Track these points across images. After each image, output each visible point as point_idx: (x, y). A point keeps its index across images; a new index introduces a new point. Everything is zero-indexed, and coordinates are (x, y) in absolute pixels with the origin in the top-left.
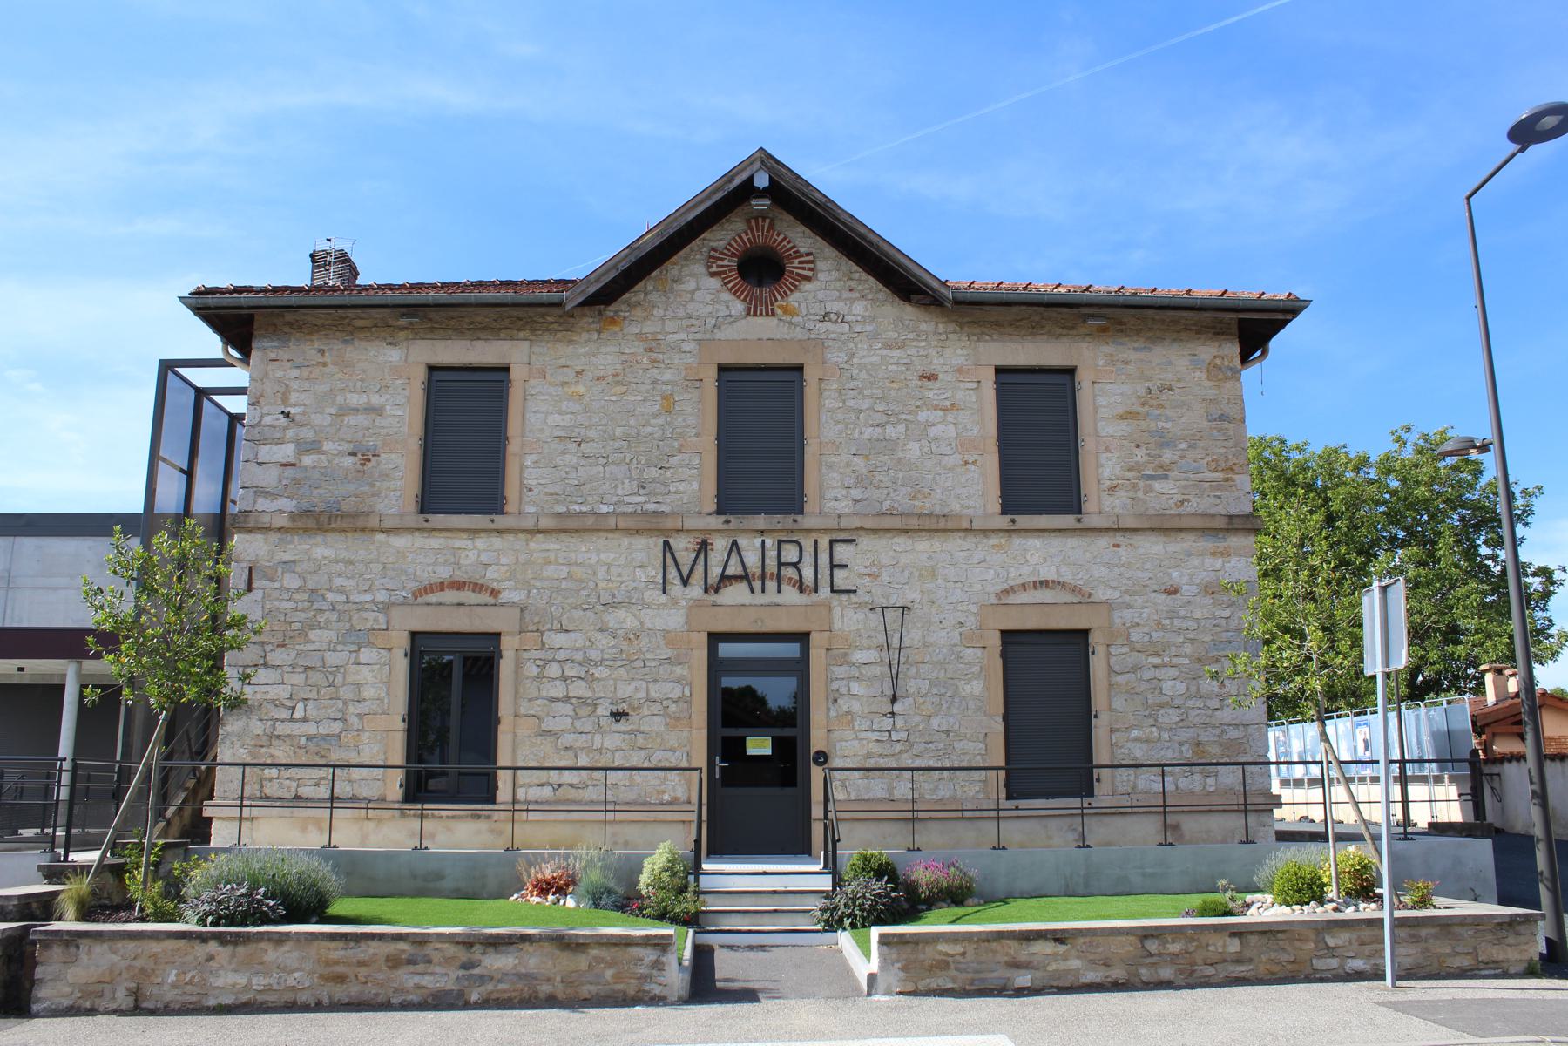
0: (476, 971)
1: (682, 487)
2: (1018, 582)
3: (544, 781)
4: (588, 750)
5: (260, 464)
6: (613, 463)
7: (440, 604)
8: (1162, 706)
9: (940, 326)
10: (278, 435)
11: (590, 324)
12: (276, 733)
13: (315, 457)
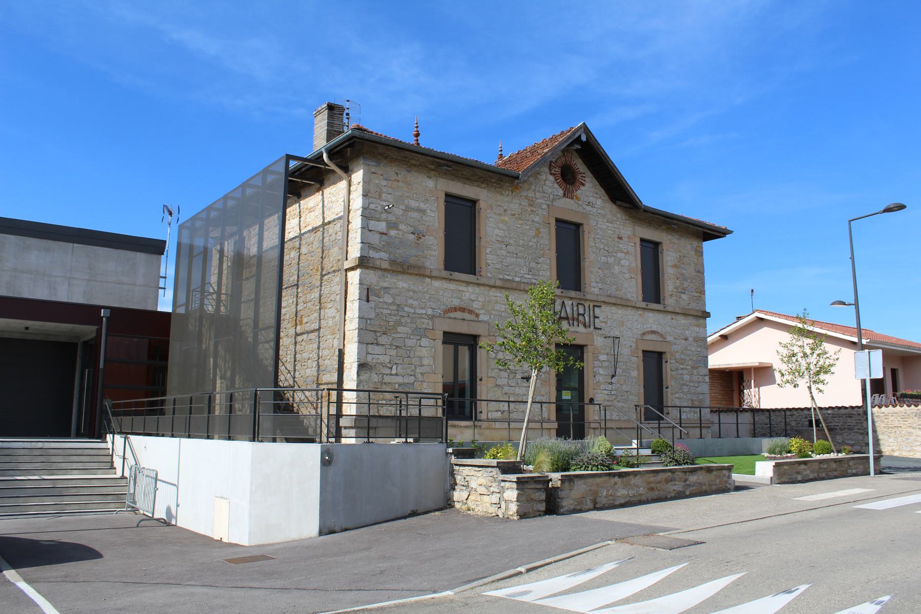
0: (687, 483)
1: (544, 273)
2: (646, 330)
3: (498, 409)
4: (514, 394)
5: (370, 231)
6: (519, 258)
7: (455, 318)
8: (684, 384)
9: (624, 216)
10: (378, 216)
11: (509, 186)
12: (384, 381)
13: (396, 232)
